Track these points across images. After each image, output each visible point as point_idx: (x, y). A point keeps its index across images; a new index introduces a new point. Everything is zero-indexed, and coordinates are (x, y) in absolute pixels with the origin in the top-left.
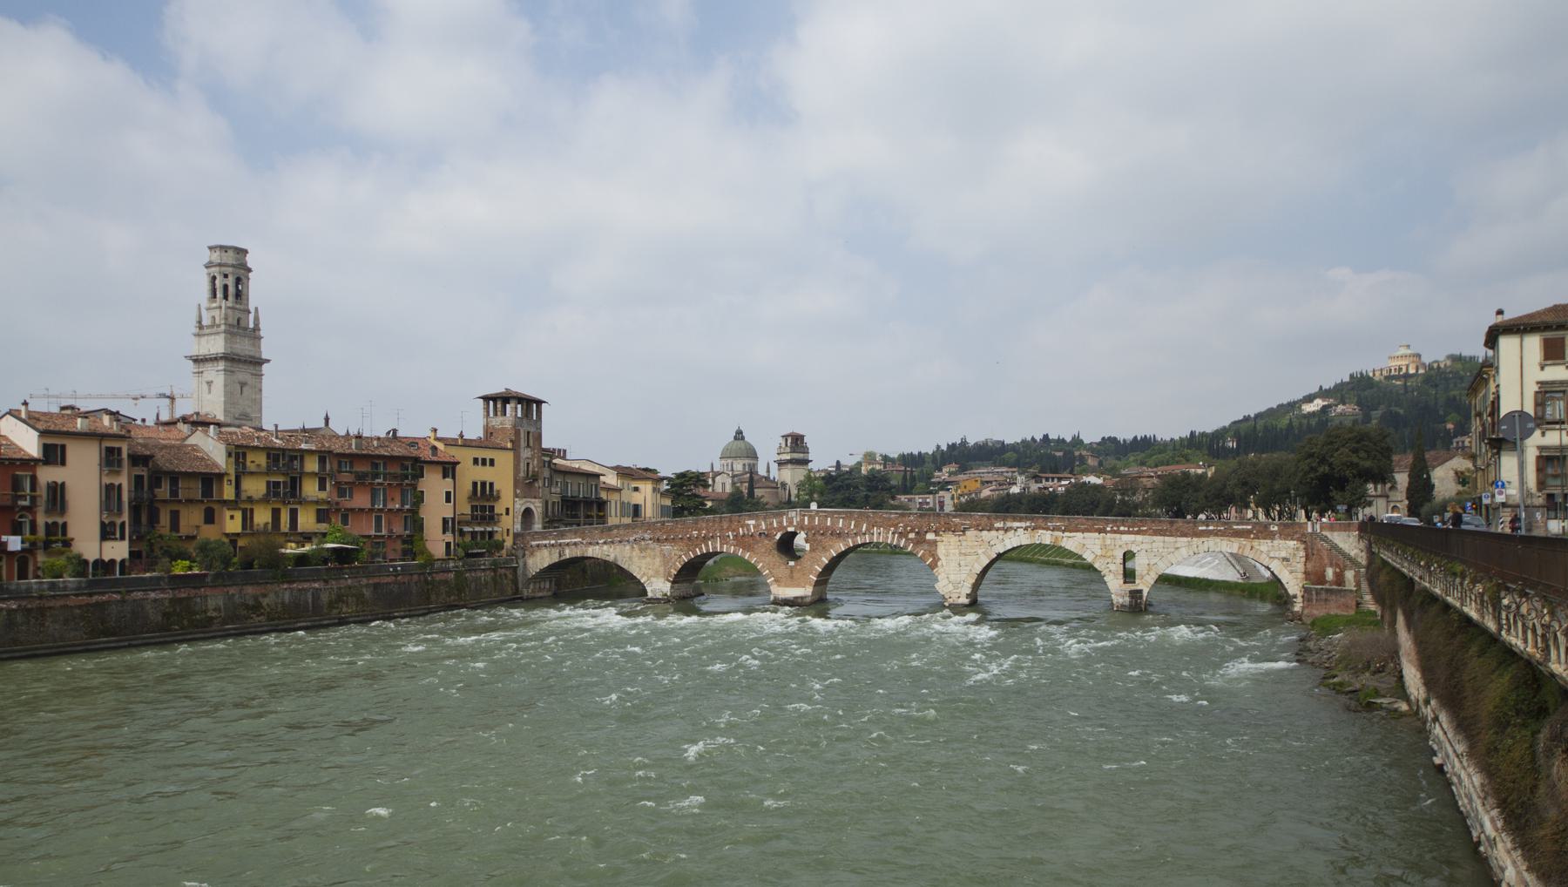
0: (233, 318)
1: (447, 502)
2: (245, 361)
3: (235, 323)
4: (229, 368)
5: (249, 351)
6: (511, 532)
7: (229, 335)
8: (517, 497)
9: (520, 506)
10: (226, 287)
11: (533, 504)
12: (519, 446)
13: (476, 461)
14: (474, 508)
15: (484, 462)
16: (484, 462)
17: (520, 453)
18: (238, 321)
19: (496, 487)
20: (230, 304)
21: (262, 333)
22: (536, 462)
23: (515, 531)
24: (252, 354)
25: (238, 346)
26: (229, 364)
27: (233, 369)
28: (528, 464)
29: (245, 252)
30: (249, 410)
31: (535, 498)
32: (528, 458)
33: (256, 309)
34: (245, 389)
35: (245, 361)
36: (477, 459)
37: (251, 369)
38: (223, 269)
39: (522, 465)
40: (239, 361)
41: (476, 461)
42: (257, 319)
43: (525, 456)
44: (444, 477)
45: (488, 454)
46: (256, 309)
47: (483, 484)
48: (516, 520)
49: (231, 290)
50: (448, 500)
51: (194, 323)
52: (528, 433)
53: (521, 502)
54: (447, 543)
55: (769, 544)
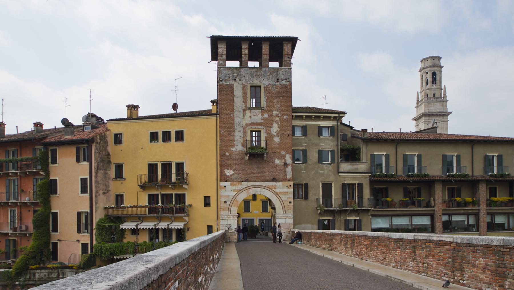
0: (431, 94)
1: (82, 192)
2: (437, 115)
3: (432, 96)
4: (427, 120)
5: (439, 109)
7: (427, 104)
8: (220, 181)
11: (266, 188)
12: (233, 110)
13: (154, 137)
14: (153, 199)
15: (167, 136)
16: (167, 136)
17: (233, 118)
18: (434, 95)
19: (186, 169)
21: (448, 99)
22: (275, 128)
24: (441, 110)
25: (433, 108)
26: (427, 118)
27: (429, 120)
29: (439, 58)
31: (274, 180)
32: (253, 124)
33: (445, 86)
36: (157, 133)
37: (441, 119)
39: (238, 135)
40: (433, 115)
41: (154, 137)
42: (445, 91)
43: (247, 120)
44: (78, 160)
46: (445, 86)
50: (84, 190)
51: (416, 102)
53: (239, 187)
54: (83, 244)
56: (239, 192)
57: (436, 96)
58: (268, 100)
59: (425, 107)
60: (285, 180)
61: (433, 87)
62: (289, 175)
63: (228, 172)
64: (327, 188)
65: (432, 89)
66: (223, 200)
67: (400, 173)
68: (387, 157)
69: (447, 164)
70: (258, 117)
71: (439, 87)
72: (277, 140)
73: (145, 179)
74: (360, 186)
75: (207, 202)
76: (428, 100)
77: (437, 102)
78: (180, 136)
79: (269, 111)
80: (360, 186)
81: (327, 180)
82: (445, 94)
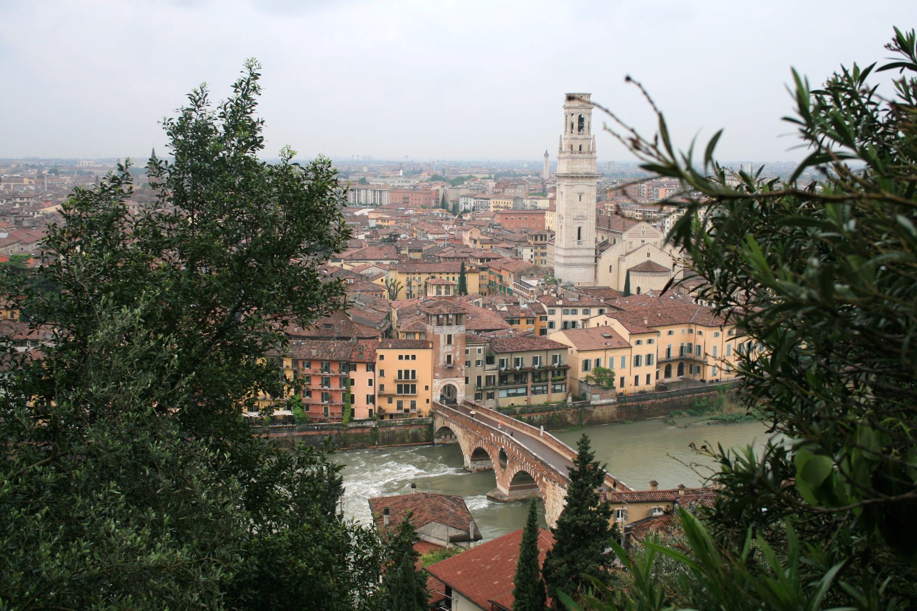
6: (430, 401)
7: (570, 160)
9: (439, 384)
10: (572, 125)
11: (455, 381)
12: (439, 346)
14: (399, 387)
15: (407, 357)
16: (407, 357)
20: (574, 136)
22: (458, 354)
23: (434, 400)
24: (589, 171)
25: (578, 166)
26: (570, 180)
28: (449, 357)
30: (585, 213)
31: (457, 377)
34: (582, 197)
35: (582, 177)
37: (588, 182)
38: (570, 110)
41: (401, 357)
42: (594, 144)
43: (446, 350)
44: (367, 371)
45: (410, 352)
46: (594, 136)
47: (407, 372)
48: (434, 393)
49: (576, 125)
51: (558, 149)
52: (449, 337)
53: (441, 381)
55: (496, 453)
56: (441, 383)
57: (583, 149)
58: (455, 341)
59: (568, 165)
60: (462, 377)
61: (579, 137)
62: (463, 375)
63: (437, 375)
64: (479, 378)
65: (577, 139)
66: (434, 387)
67: (513, 367)
68: (507, 359)
69: (535, 360)
70: (449, 349)
71: (587, 136)
72: (458, 359)
73: (397, 378)
74: (494, 376)
75: (427, 388)
76: (573, 155)
77: (583, 158)
78: (414, 357)
79: (456, 345)
80: (494, 376)
81: (479, 375)
82: (594, 148)
